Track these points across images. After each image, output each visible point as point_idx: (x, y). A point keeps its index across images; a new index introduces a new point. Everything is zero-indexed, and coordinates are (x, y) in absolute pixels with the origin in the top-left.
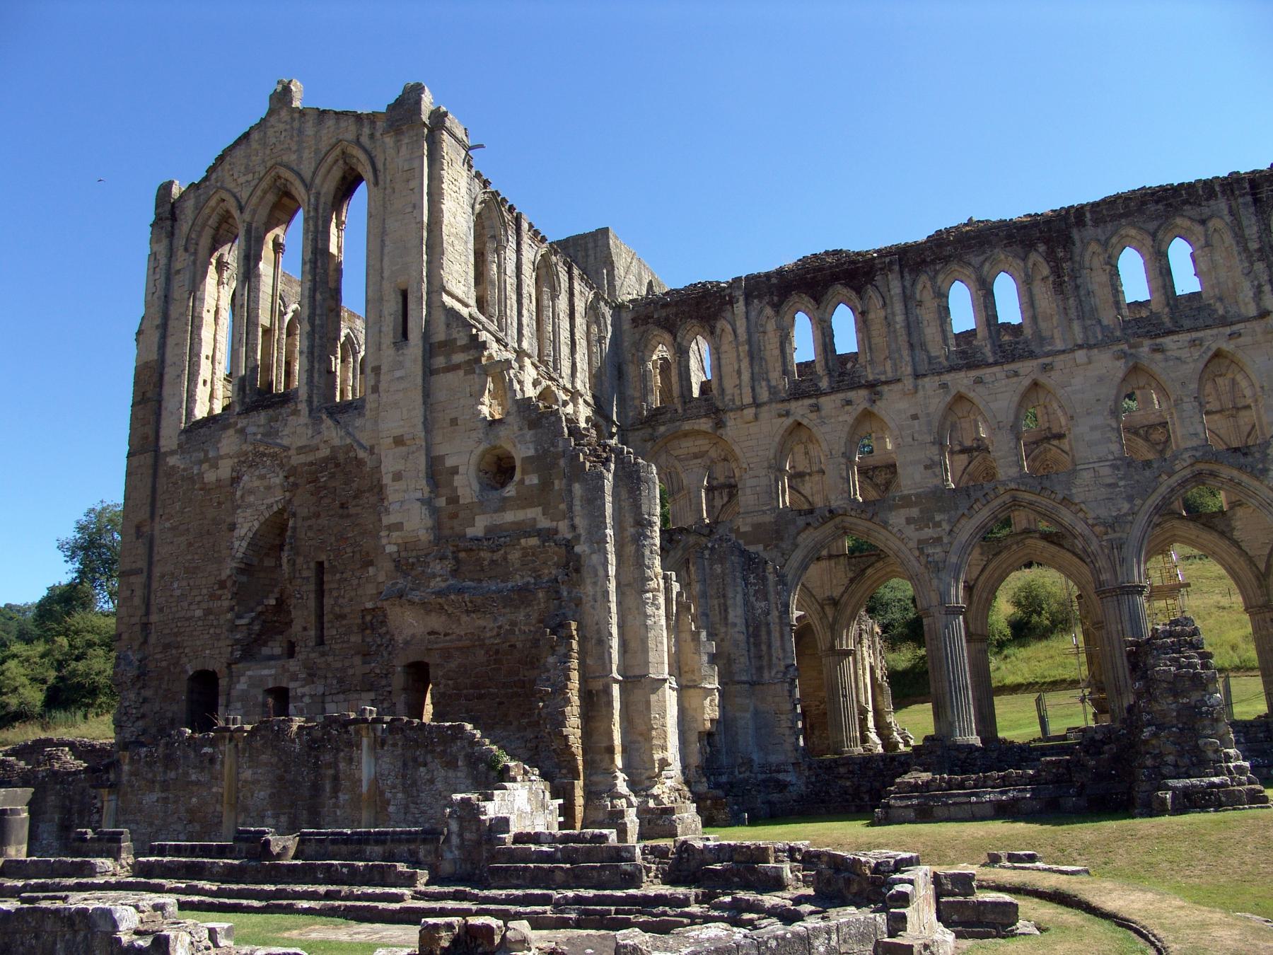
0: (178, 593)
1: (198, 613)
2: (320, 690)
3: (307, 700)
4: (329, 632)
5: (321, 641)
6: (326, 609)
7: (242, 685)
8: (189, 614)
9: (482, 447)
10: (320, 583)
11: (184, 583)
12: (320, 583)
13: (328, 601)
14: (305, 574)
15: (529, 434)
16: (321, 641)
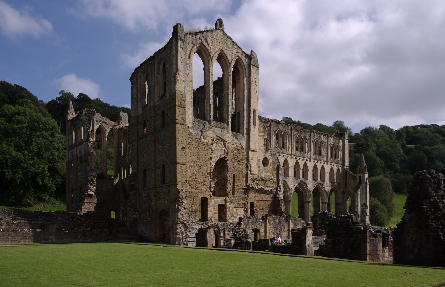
0: (195, 173)
1: (202, 180)
2: (234, 206)
3: (231, 208)
4: (236, 192)
5: (233, 194)
6: (235, 186)
7: (213, 203)
8: (199, 180)
9: (264, 157)
10: (234, 180)
11: (197, 171)
12: (234, 180)
13: (235, 184)
14: (231, 176)
15: (272, 157)
16: (233, 194)
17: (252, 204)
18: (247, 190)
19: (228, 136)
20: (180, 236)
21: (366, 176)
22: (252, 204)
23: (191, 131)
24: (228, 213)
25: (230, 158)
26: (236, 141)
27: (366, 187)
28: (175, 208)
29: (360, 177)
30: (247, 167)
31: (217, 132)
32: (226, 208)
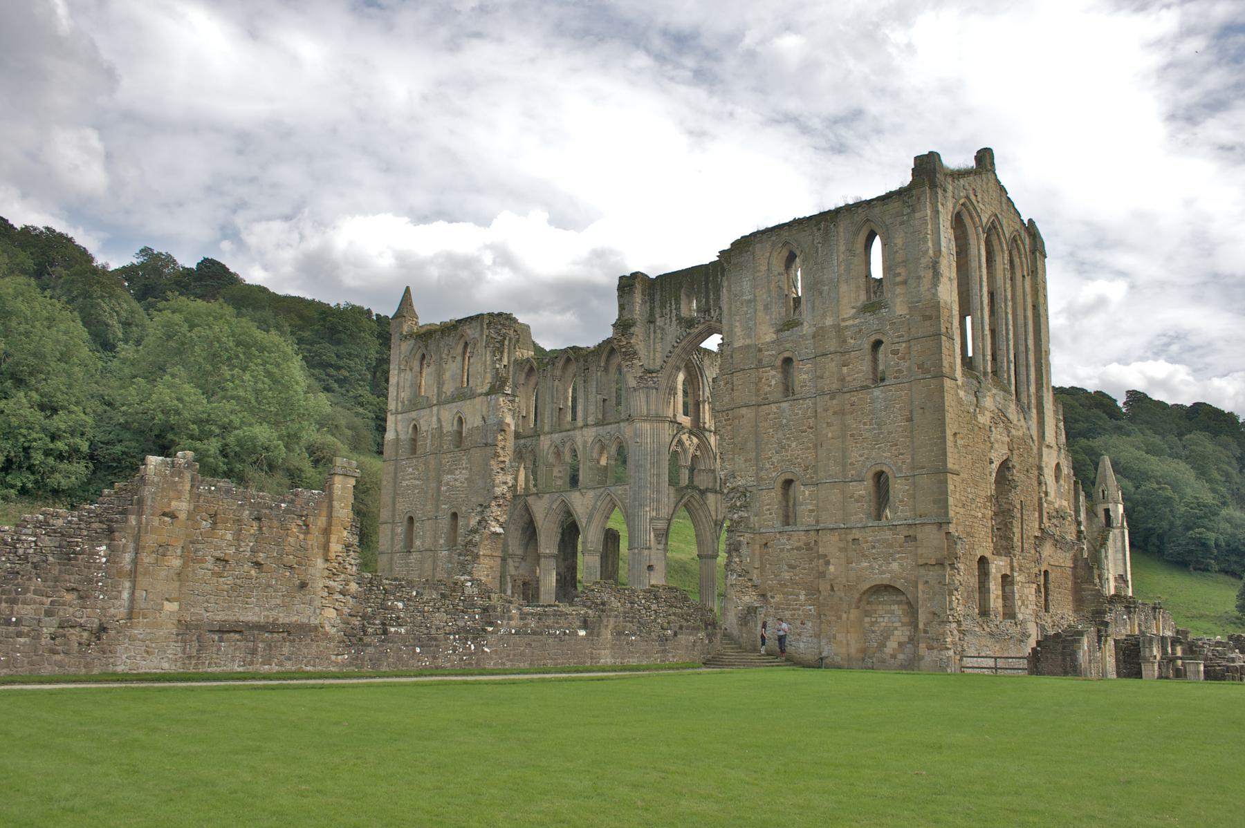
17: (1046, 572)
18: (1039, 541)
19: (1012, 411)
20: (951, 653)
21: (1121, 508)
22: (1046, 572)
23: (962, 393)
24: (1017, 596)
25: (1015, 460)
26: (1022, 422)
27: (1123, 533)
28: (941, 583)
29: (1107, 511)
30: (1040, 484)
31: (998, 398)
32: (1012, 583)
